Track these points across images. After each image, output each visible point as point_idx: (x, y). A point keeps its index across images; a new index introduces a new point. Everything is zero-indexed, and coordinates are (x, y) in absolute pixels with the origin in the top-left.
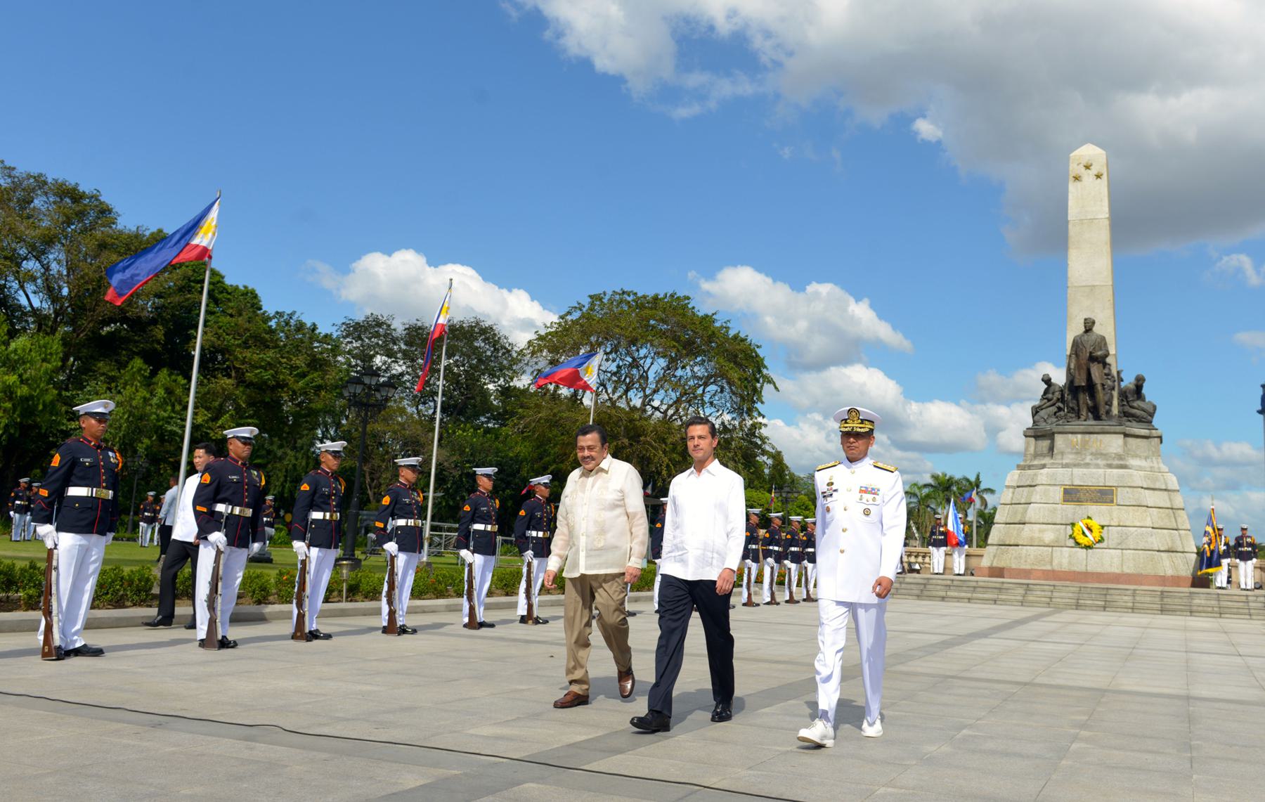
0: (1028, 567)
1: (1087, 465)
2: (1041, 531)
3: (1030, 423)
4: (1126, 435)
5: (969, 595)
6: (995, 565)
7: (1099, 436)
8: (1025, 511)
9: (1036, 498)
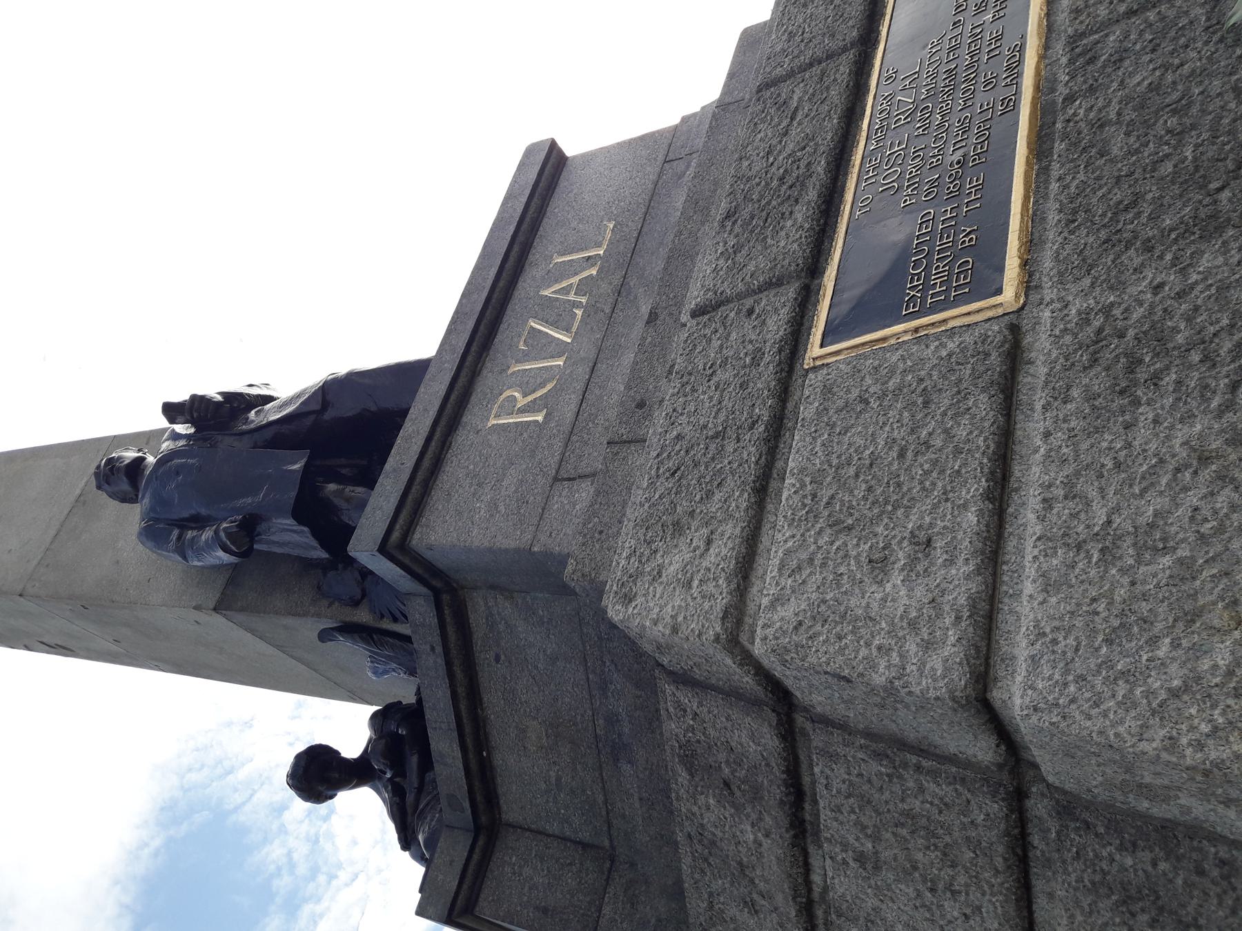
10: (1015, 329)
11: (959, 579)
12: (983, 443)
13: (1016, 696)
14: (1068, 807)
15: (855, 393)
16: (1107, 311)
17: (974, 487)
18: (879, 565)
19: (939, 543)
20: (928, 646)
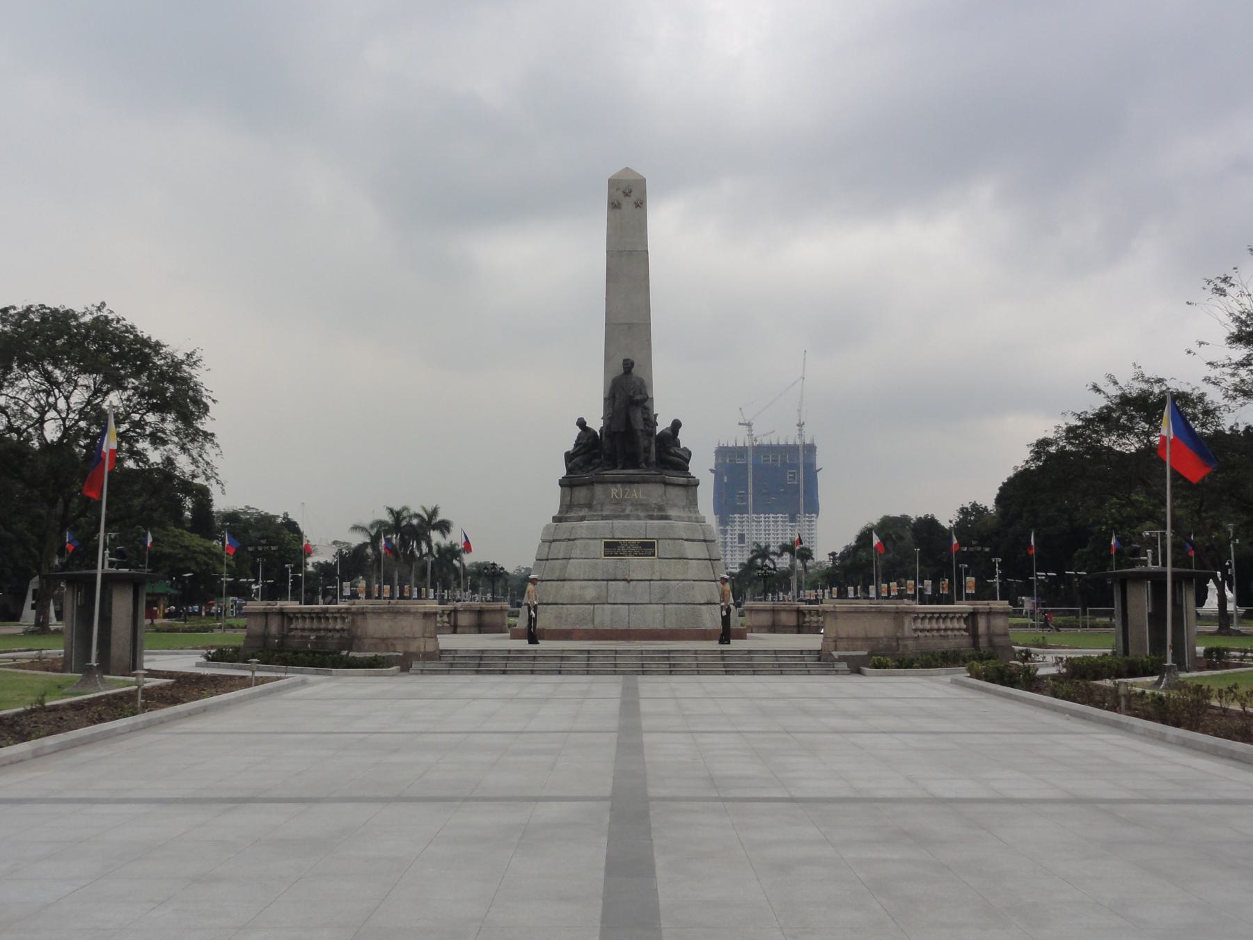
0: (569, 627)
1: (627, 517)
2: (582, 588)
3: (563, 472)
4: (666, 484)
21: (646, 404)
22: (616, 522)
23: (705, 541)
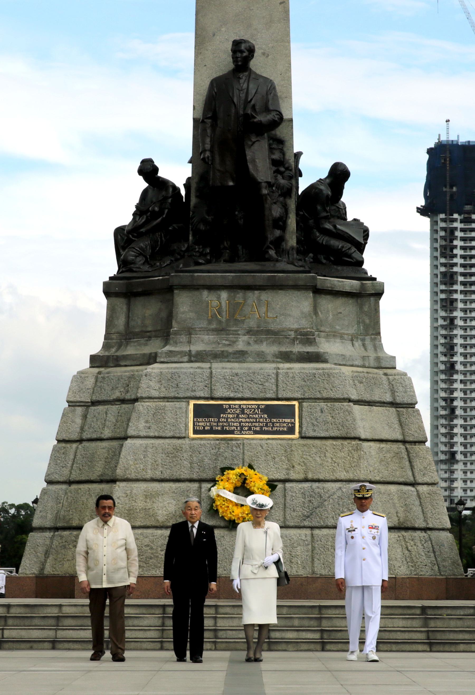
1: (241, 356)
2: (148, 496)
4: (318, 291)
5: (50, 634)
6: (48, 570)
7: (265, 296)
8: (116, 454)
9: (137, 426)
10: (184, 438)
11: (143, 434)
12: (164, 435)
13: (129, 441)
14: (122, 445)
15: (178, 413)
16: (182, 450)
17: (157, 434)
18: (147, 422)
19: (149, 430)
20: (134, 430)
21: (280, 132)
22: (219, 367)
23: (393, 404)
